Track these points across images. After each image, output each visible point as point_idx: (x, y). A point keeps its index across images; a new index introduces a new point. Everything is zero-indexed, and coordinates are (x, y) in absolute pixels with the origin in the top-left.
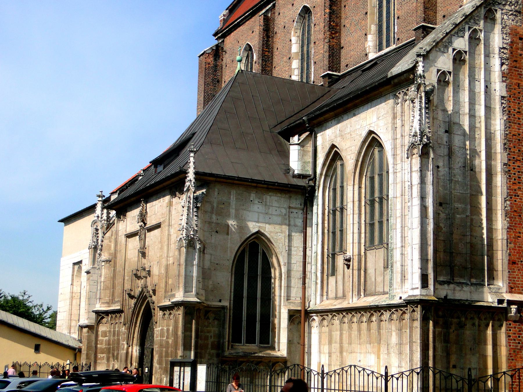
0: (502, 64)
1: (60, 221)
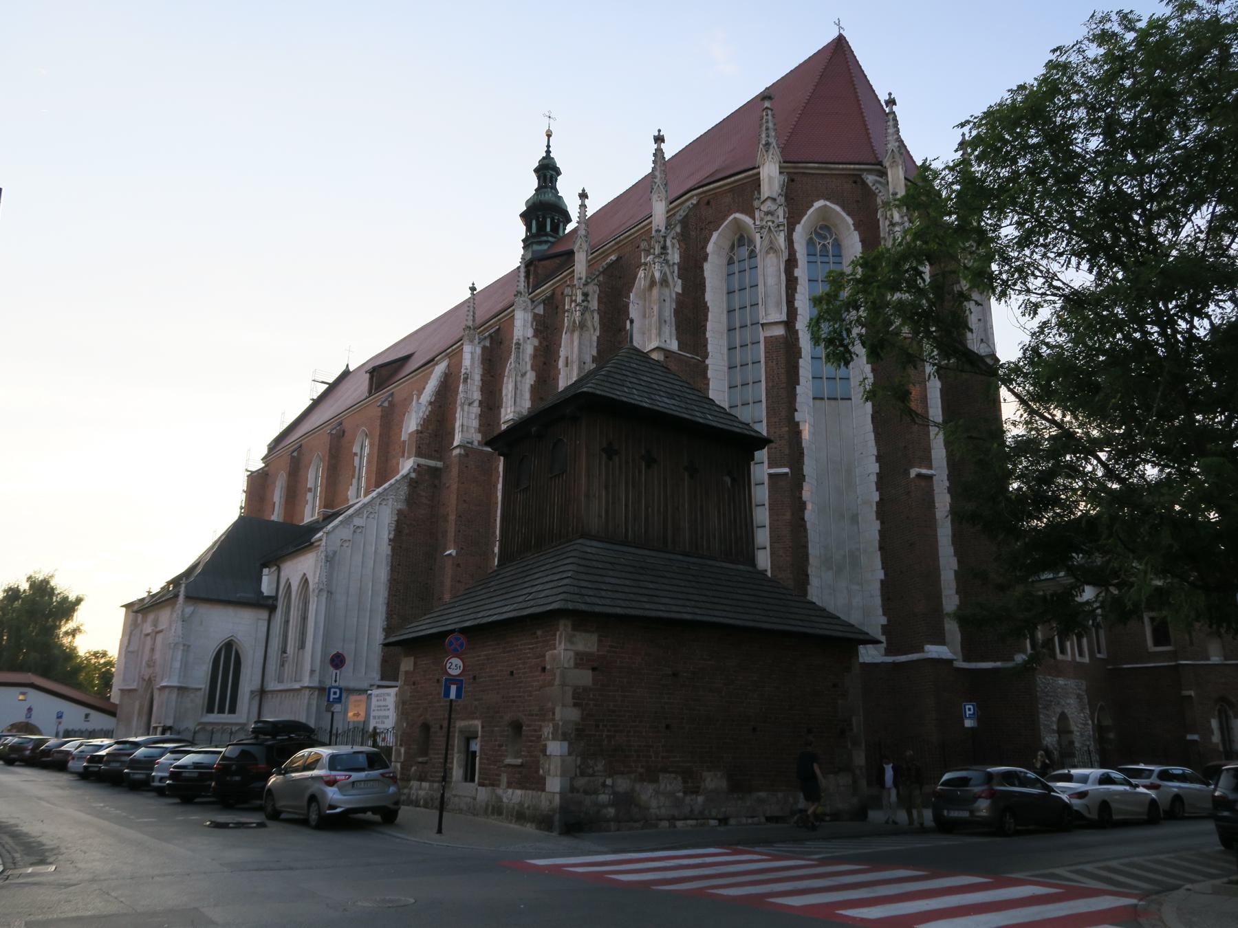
0: (389, 534)
1: (122, 606)
